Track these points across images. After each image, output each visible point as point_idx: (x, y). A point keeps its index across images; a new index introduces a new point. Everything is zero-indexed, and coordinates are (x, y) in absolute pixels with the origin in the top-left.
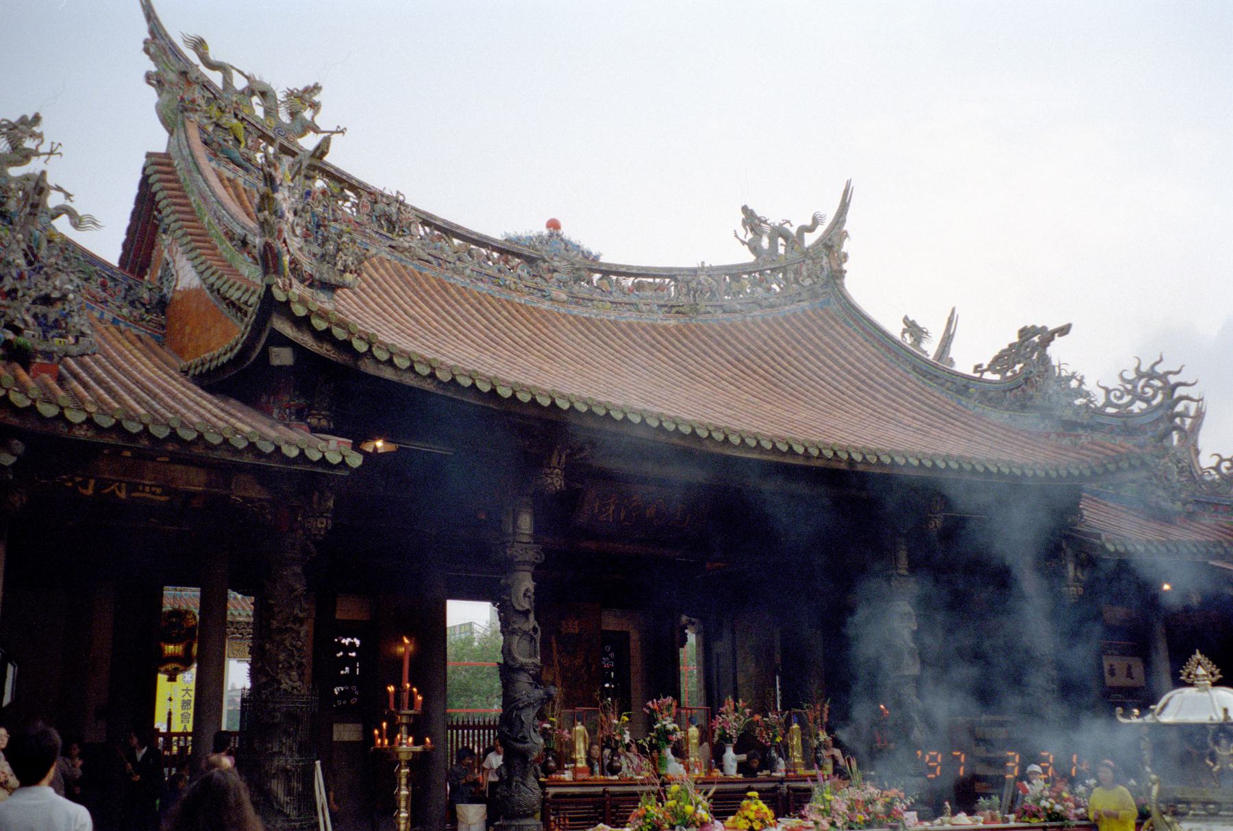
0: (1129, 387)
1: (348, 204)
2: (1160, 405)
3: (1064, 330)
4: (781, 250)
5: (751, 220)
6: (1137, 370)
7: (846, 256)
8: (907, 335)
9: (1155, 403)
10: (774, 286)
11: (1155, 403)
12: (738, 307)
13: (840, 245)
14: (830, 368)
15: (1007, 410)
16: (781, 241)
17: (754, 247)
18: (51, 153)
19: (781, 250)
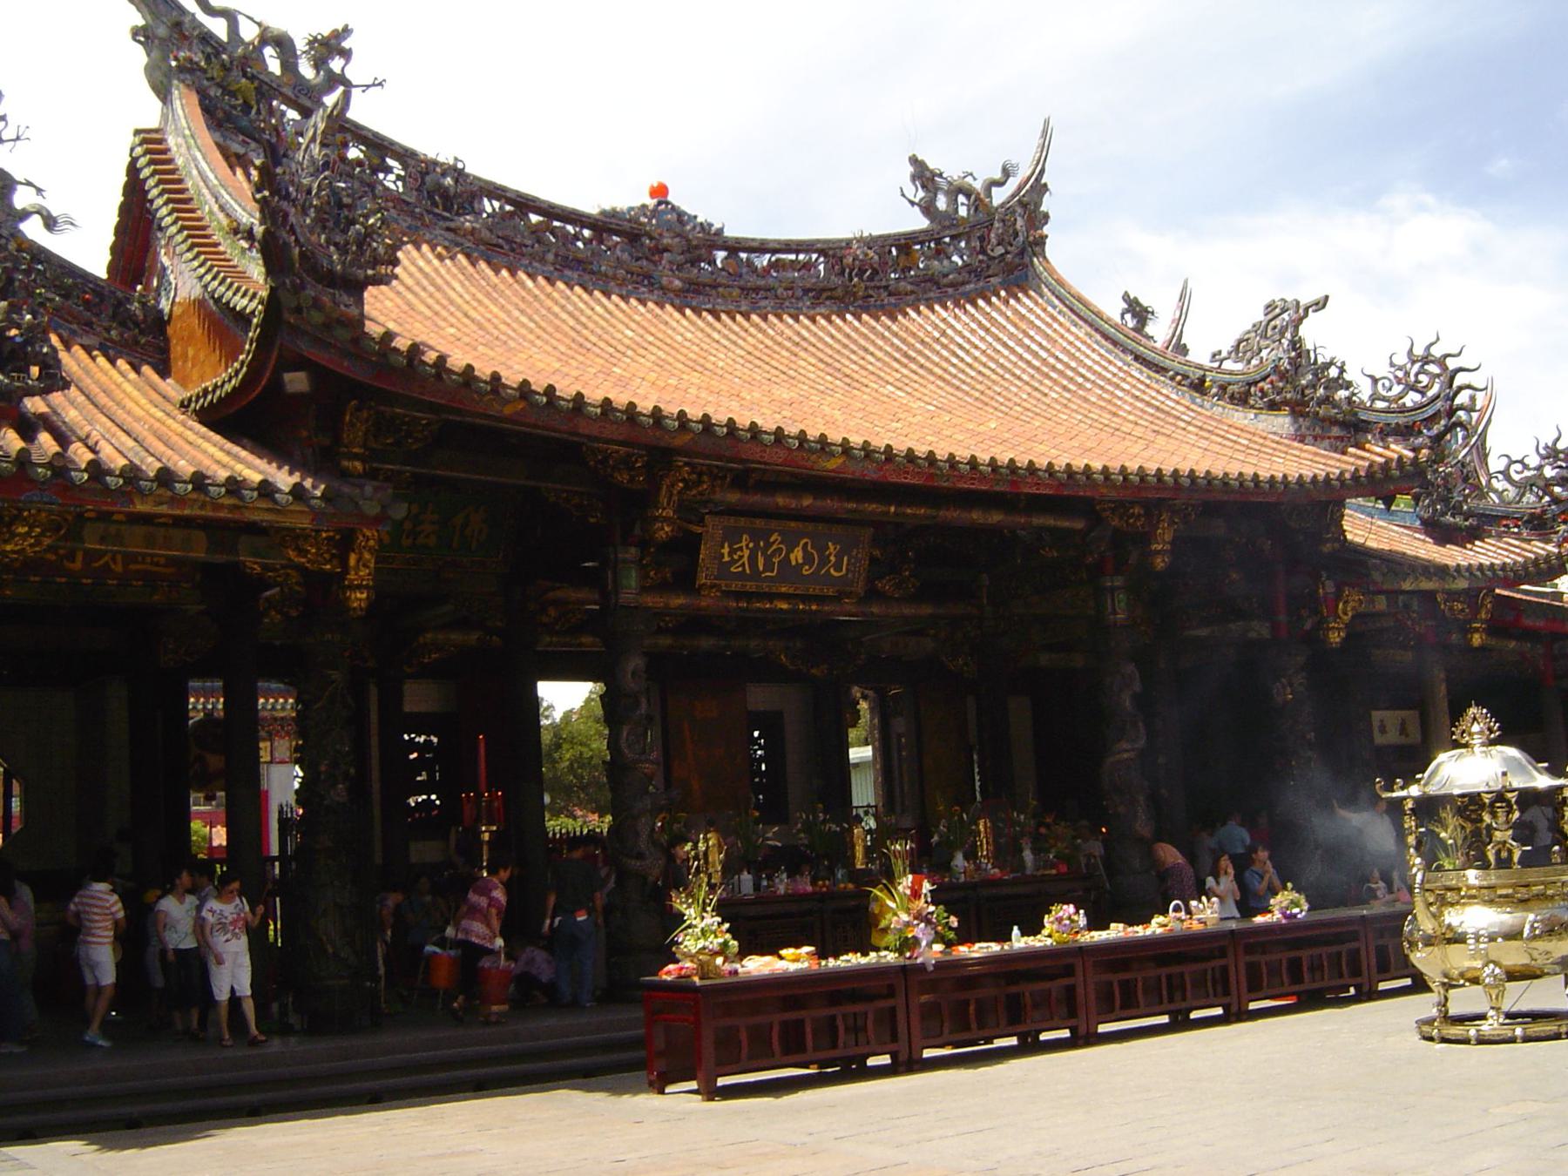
1: (392, 177)
2: (1437, 397)
3: (1321, 304)
4: (963, 212)
5: (924, 175)
7: (1046, 217)
8: (1128, 317)
10: (955, 258)
11: (1430, 393)
12: (909, 288)
13: (1038, 204)
14: (1028, 362)
15: (1252, 407)
16: (961, 199)
17: (928, 208)
18: (18, 138)
19: (963, 212)
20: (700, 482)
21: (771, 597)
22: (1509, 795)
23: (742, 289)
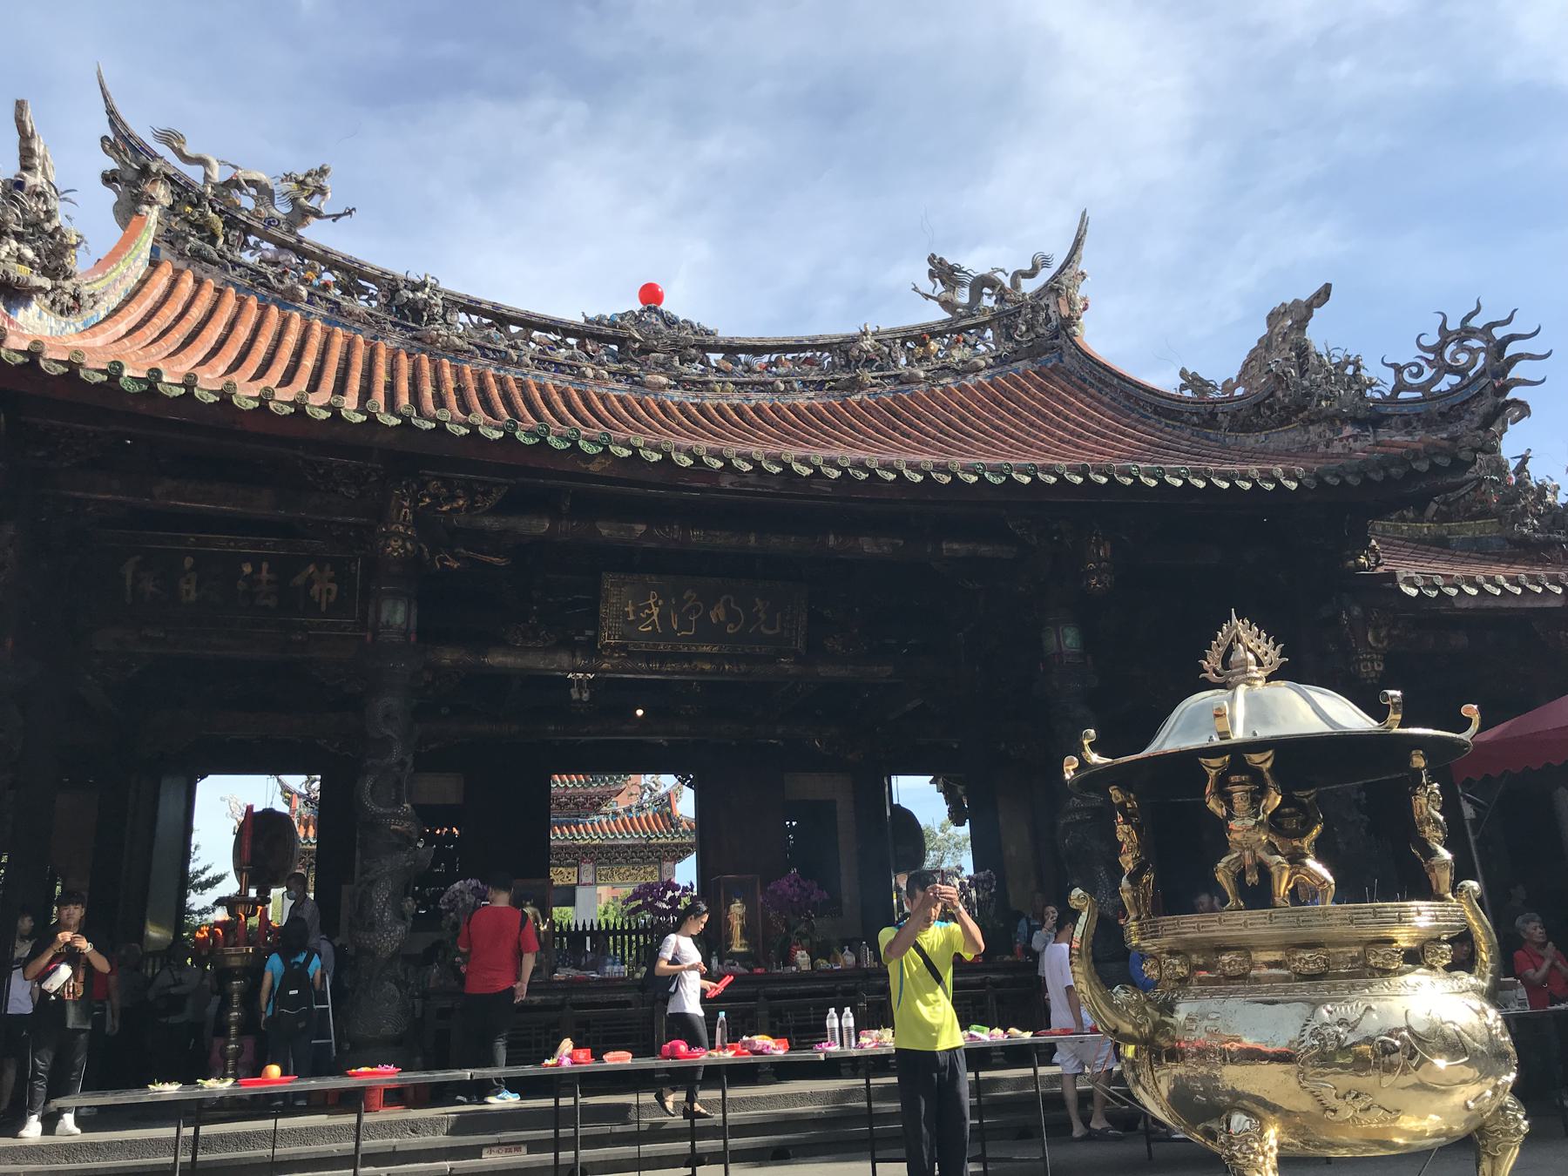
0: (1431, 357)
2: (1482, 373)
3: (1324, 294)
6: (1443, 328)
9: (1471, 373)
17: (946, 305)
20: (454, 498)
21: (689, 657)
22: (1256, 758)
23: (735, 383)
